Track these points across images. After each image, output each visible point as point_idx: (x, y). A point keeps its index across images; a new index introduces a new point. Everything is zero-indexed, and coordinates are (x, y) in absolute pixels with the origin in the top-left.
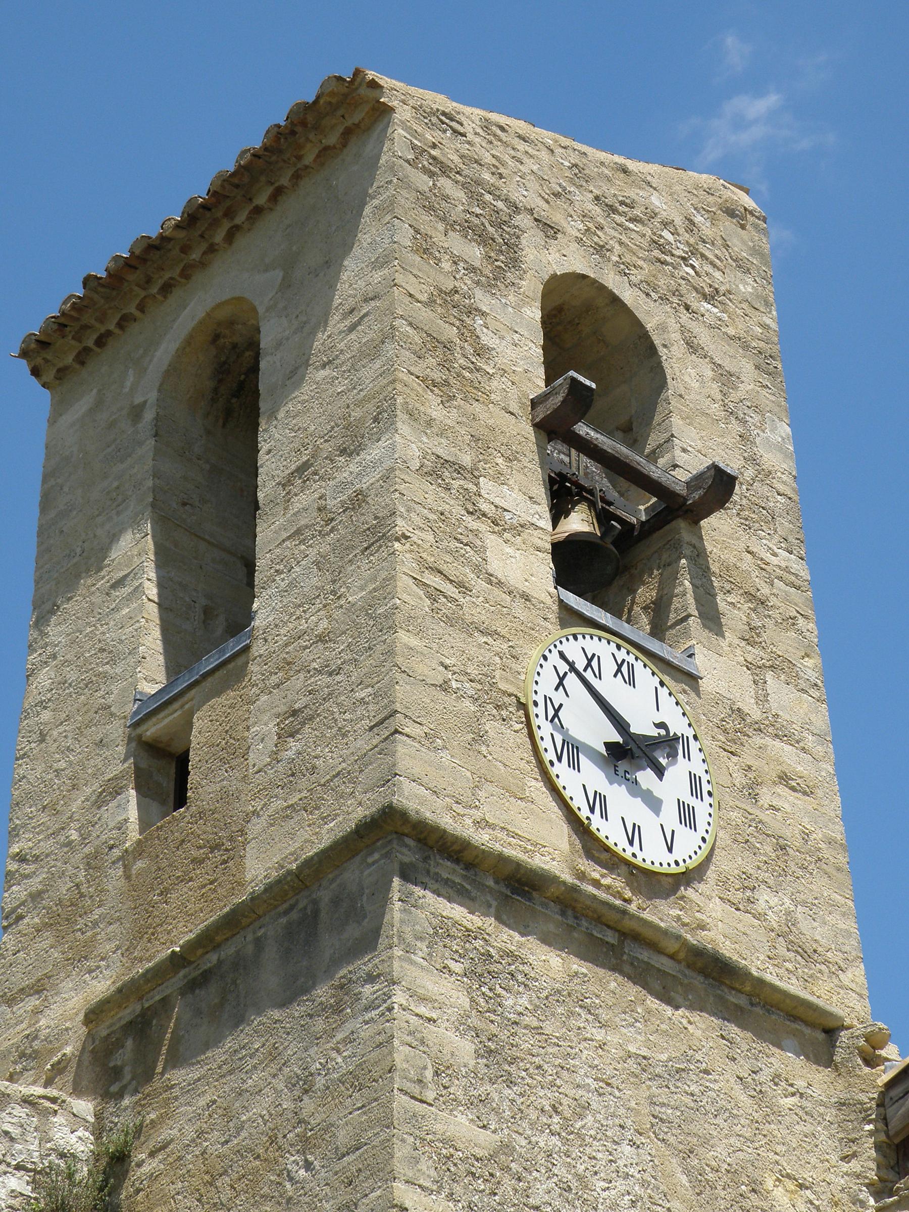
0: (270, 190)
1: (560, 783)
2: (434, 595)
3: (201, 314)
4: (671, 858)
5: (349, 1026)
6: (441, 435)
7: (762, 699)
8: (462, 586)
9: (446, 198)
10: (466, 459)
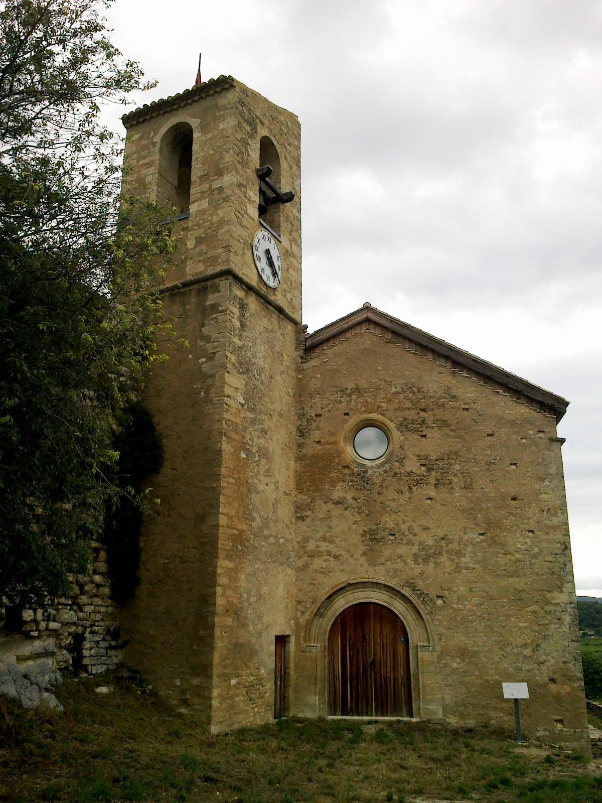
0: (198, 97)
1: (257, 265)
2: (238, 217)
3: (175, 123)
4: (274, 284)
5: (215, 316)
6: (241, 176)
7: (291, 248)
8: (243, 217)
9: (244, 113)
10: (245, 183)
